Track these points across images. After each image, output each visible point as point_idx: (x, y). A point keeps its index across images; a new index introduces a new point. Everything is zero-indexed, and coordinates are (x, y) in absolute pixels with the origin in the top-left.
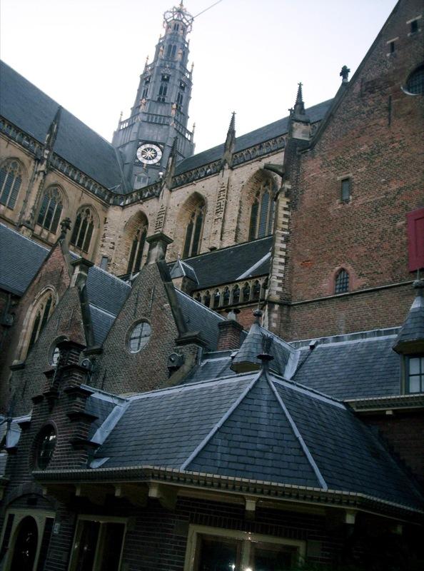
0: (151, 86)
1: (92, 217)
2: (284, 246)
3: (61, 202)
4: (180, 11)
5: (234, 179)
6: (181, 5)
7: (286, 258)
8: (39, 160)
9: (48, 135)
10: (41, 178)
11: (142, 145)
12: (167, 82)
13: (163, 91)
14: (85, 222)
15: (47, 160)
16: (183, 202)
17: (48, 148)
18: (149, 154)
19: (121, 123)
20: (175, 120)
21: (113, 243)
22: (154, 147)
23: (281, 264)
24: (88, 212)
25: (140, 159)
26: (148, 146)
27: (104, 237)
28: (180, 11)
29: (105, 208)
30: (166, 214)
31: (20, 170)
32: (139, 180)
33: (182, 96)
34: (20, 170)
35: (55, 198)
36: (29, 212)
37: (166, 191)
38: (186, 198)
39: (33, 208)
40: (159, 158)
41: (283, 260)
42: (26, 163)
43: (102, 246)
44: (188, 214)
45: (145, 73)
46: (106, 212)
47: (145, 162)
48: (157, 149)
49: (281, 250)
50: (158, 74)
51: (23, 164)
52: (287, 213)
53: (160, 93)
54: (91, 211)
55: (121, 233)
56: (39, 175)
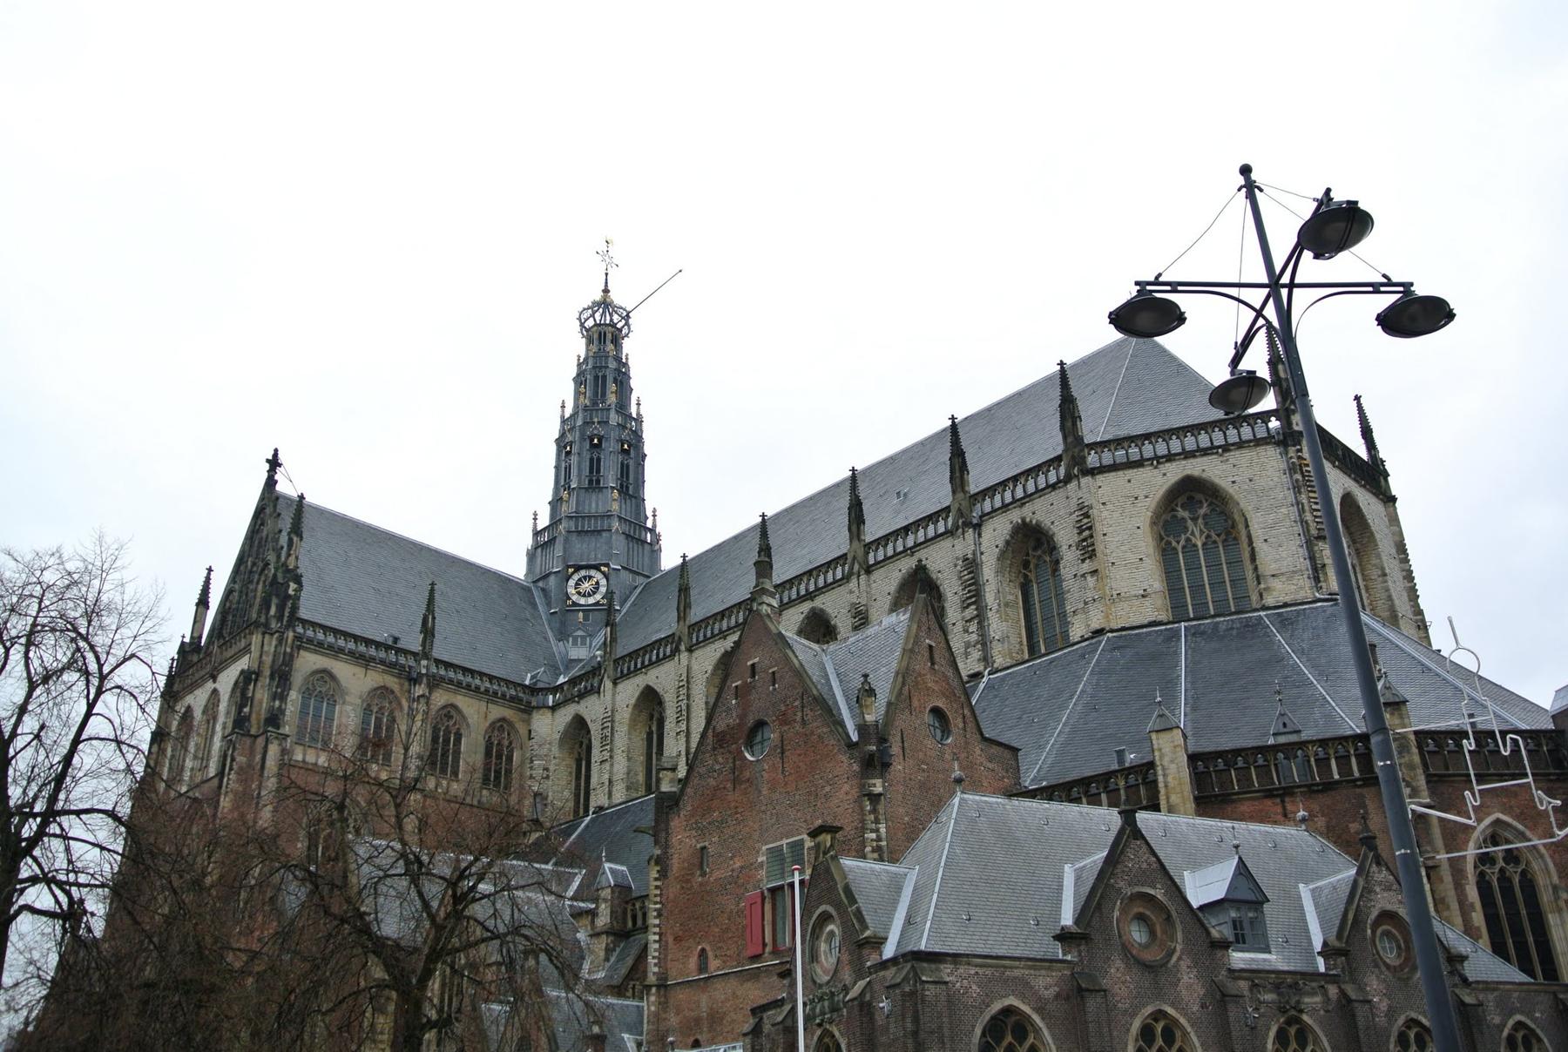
0: (574, 459)
4: (605, 304)
5: (695, 667)
6: (606, 291)
8: (414, 681)
12: (602, 442)
13: (595, 466)
16: (633, 701)
18: (586, 586)
19: (536, 533)
20: (620, 518)
22: (593, 572)
25: (574, 598)
26: (583, 573)
28: (605, 304)
29: (525, 716)
30: (613, 721)
32: (575, 643)
36: (414, 764)
37: (608, 684)
38: (637, 694)
42: (396, 688)
44: (644, 716)
45: (563, 435)
46: (528, 722)
47: (582, 601)
50: (582, 438)
55: (555, 750)
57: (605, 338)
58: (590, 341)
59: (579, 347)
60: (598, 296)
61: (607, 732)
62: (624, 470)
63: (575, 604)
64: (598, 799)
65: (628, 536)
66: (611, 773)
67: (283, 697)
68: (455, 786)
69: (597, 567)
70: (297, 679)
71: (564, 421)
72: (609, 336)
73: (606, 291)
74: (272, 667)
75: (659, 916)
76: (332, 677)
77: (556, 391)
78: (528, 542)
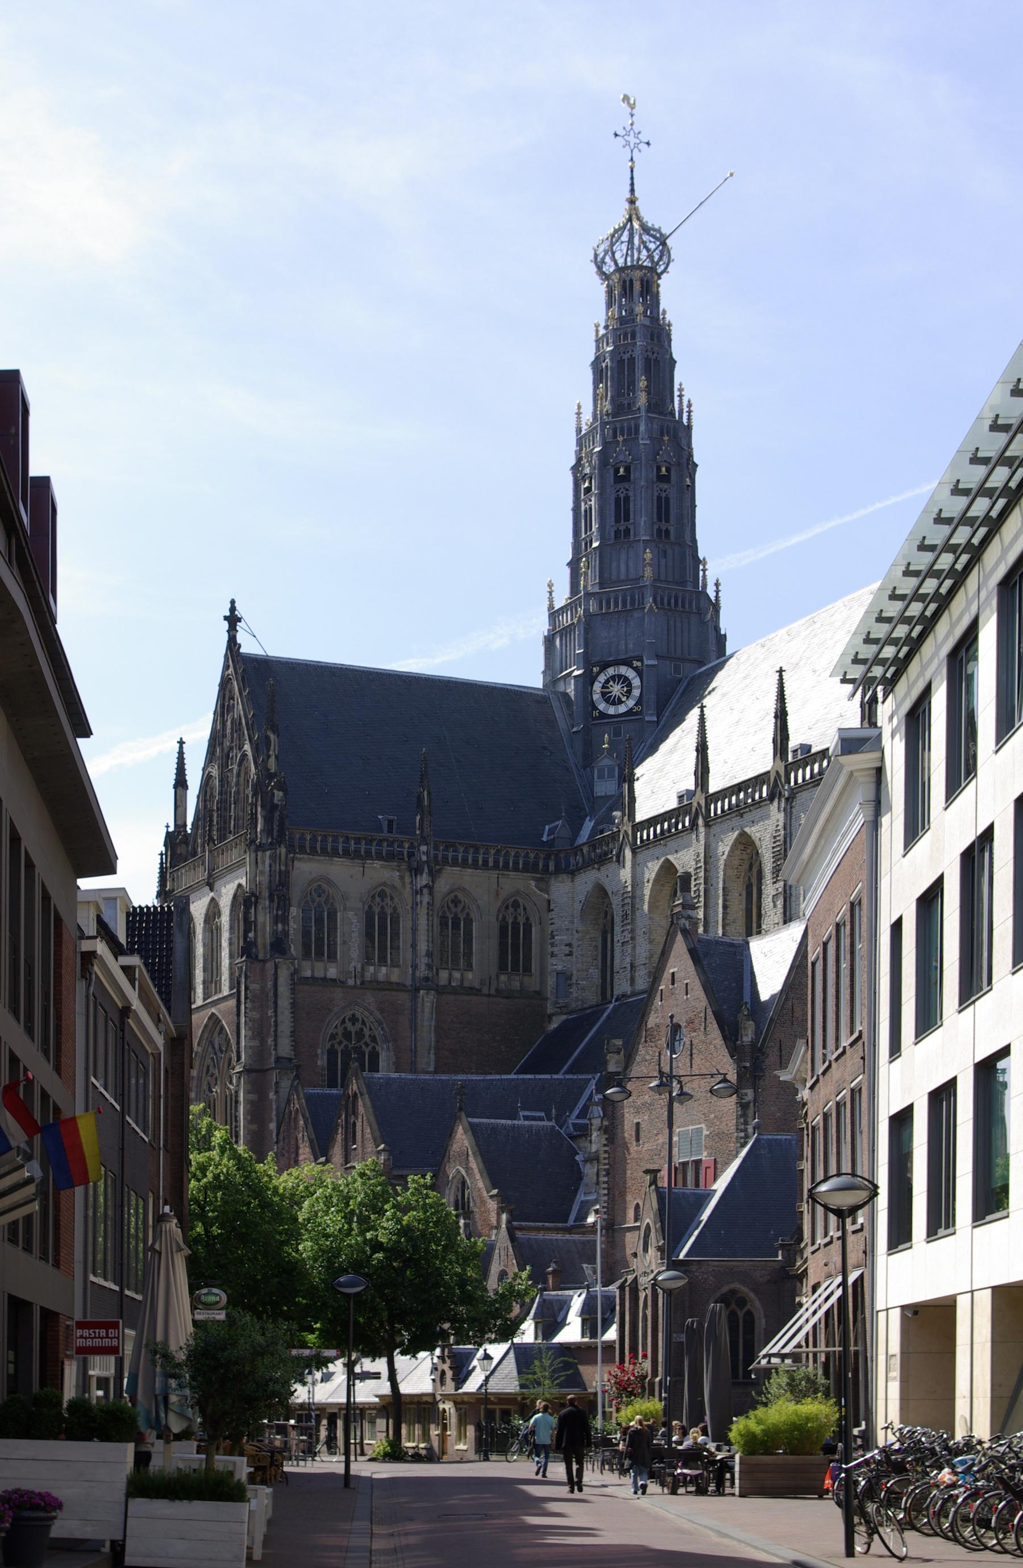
1: (525, 909)
2: (606, 1179)
3: (468, 914)
7: (608, 1189)
8: (417, 871)
9: (418, 818)
10: (426, 898)
11: (598, 674)
14: (516, 924)
15: (427, 862)
17: (424, 841)
21: (569, 945)
22: (623, 670)
23: (605, 1195)
24: (516, 905)
26: (611, 671)
27: (553, 937)
31: (392, 898)
32: (601, 776)
34: (392, 898)
35: (456, 914)
39: (429, 954)
40: (636, 693)
41: (606, 1192)
42: (397, 882)
43: (553, 955)
48: (631, 674)
49: (604, 1183)
51: (394, 887)
52: (606, 1148)
53: (617, 520)
54: (521, 901)
55: (578, 924)
56: (422, 894)
61: (628, 908)
62: (662, 509)
63: (603, 715)
64: (622, 986)
66: (633, 956)
67: (284, 919)
68: (470, 975)
69: (628, 663)
70: (296, 894)
72: (637, 286)
74: (270, 888)
75: (608, 1174)
76: (329, 882)
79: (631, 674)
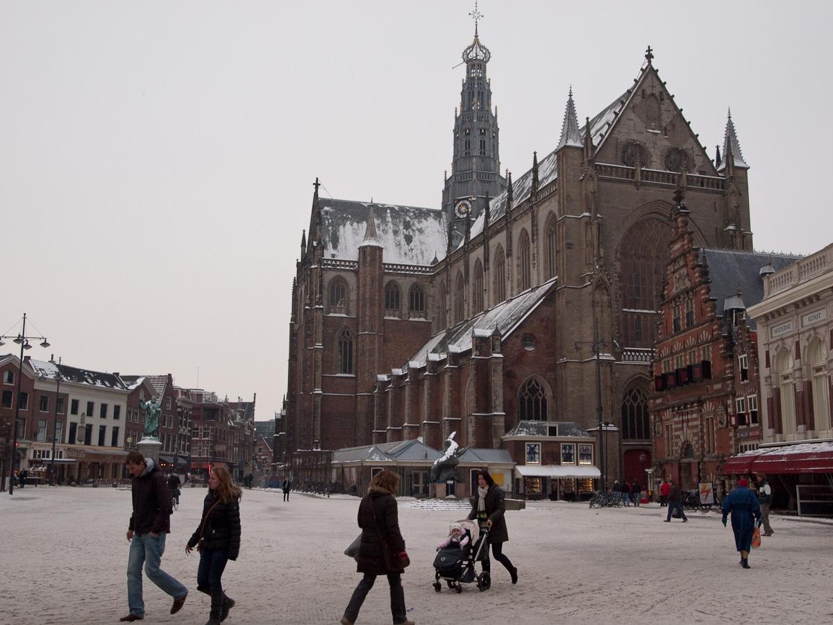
6: (476, 36)
13: (468, 145)
18: (463, 209)
26: (461, 203)
33: (484, 141)
48: (468, 203)
57: (476, 64)
58: (468, 72)
59: (462, 73)
60: (471, 43)
62: (483, 144)
63: (459, 218)
65: (481, 181)
69: (467, 199)
71: (457, 119)
73: (476, 36)
77: (453, 102)
78: (443, 186)
79: (468, 203)
